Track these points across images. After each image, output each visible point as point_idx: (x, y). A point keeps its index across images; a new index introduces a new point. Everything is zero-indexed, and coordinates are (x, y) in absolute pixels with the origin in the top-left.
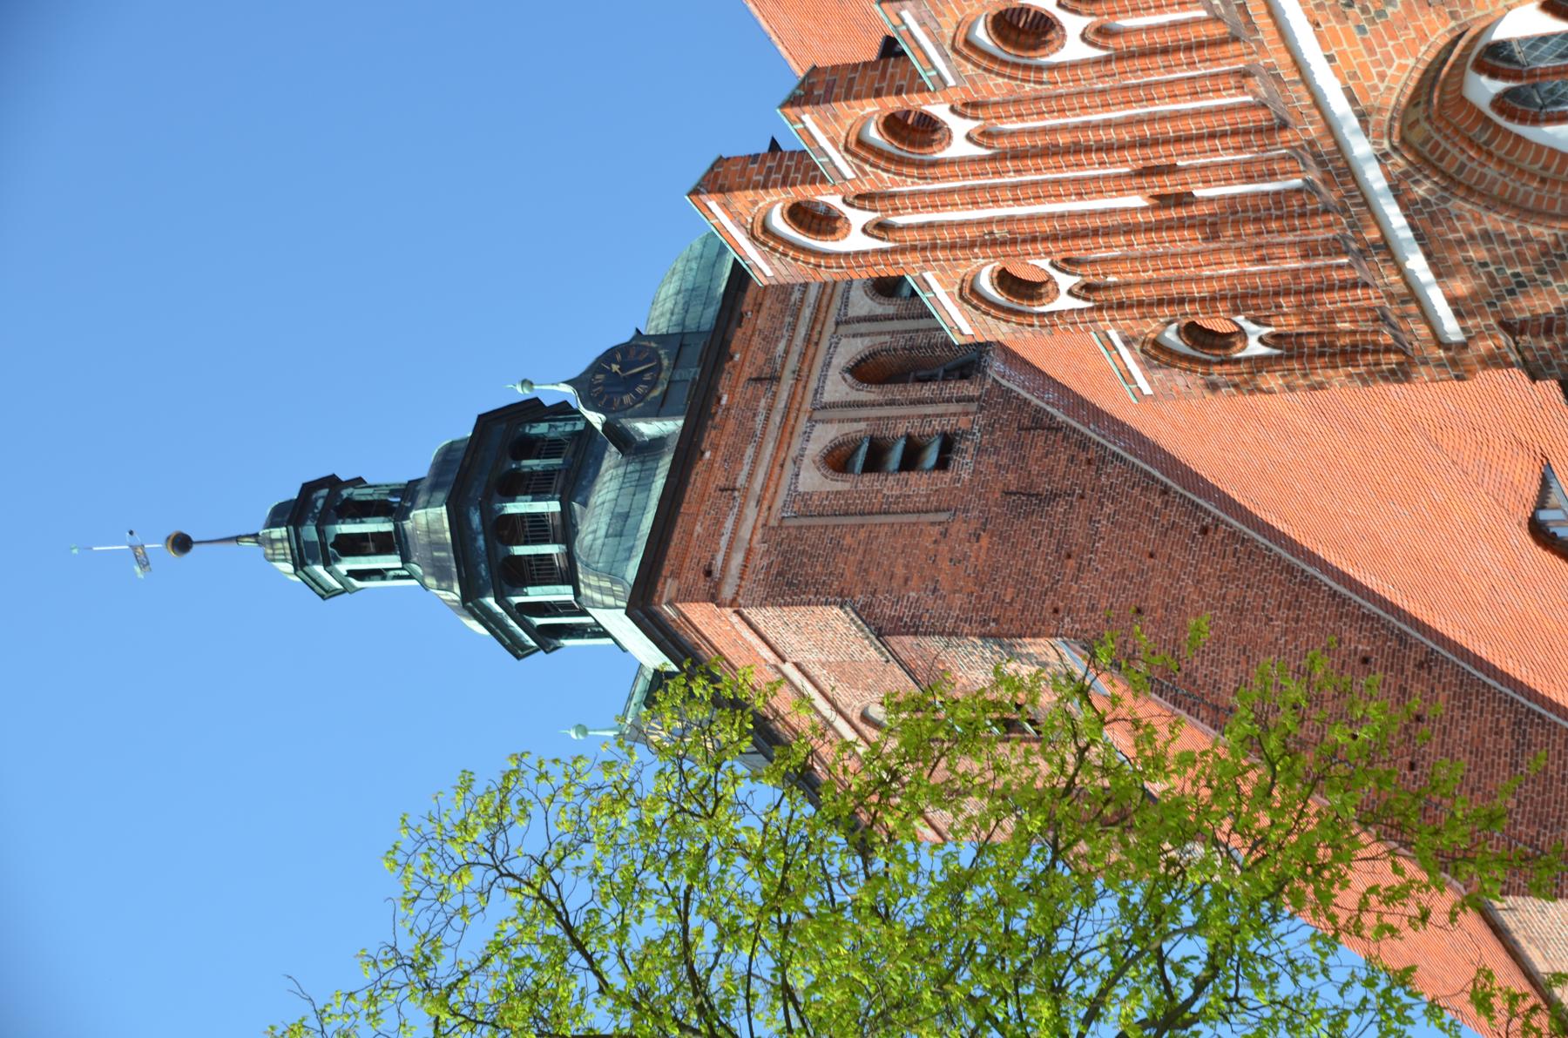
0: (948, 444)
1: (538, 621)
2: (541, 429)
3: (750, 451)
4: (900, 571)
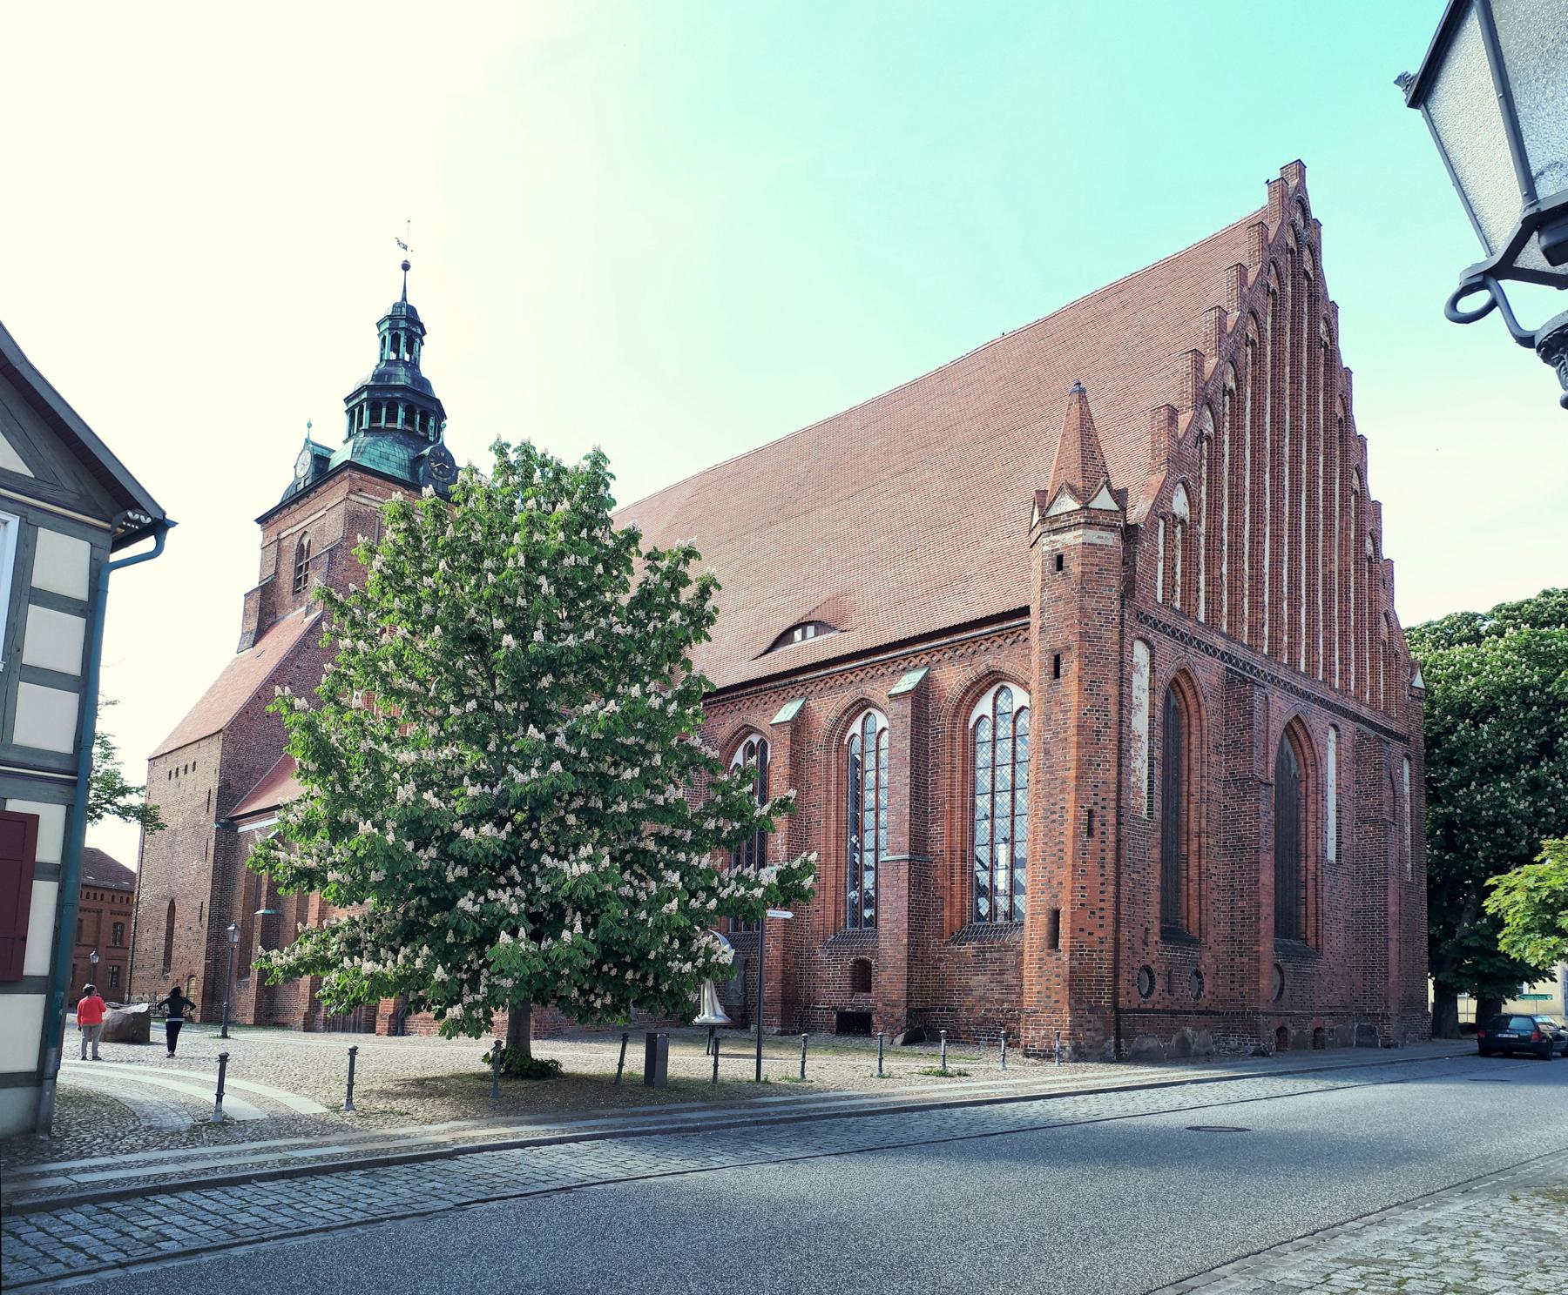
2: (432, 423)
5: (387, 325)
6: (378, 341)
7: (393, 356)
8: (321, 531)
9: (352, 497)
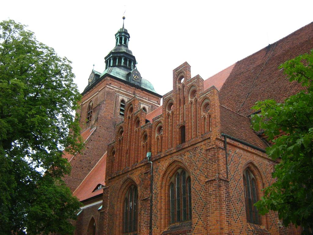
2: (132, 64)
4: (108, 108)
6: (115, 40)
8: (97, 99)
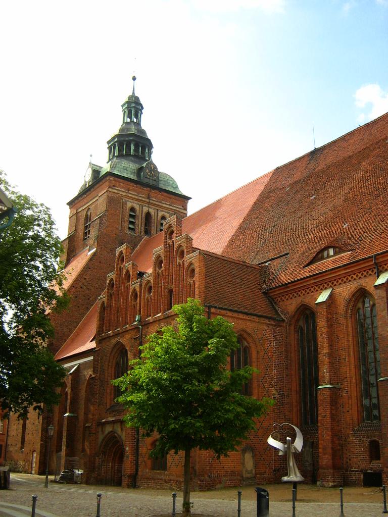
0: (133, 229)
1: (112, 147)
3: (135, 194)
4: (111, 221)
5: (126, 106)
6: (122, 114)
7: (129, 120)
8: (96, 206)
9: (110, 190)
